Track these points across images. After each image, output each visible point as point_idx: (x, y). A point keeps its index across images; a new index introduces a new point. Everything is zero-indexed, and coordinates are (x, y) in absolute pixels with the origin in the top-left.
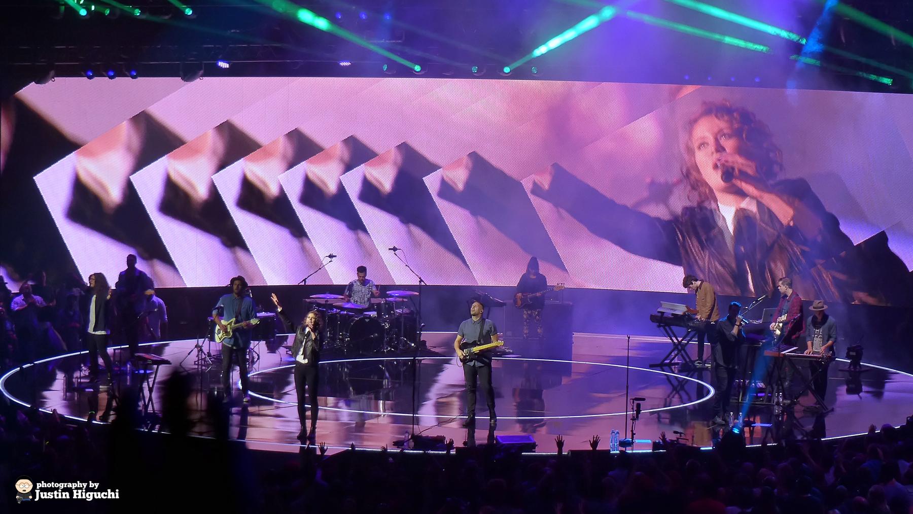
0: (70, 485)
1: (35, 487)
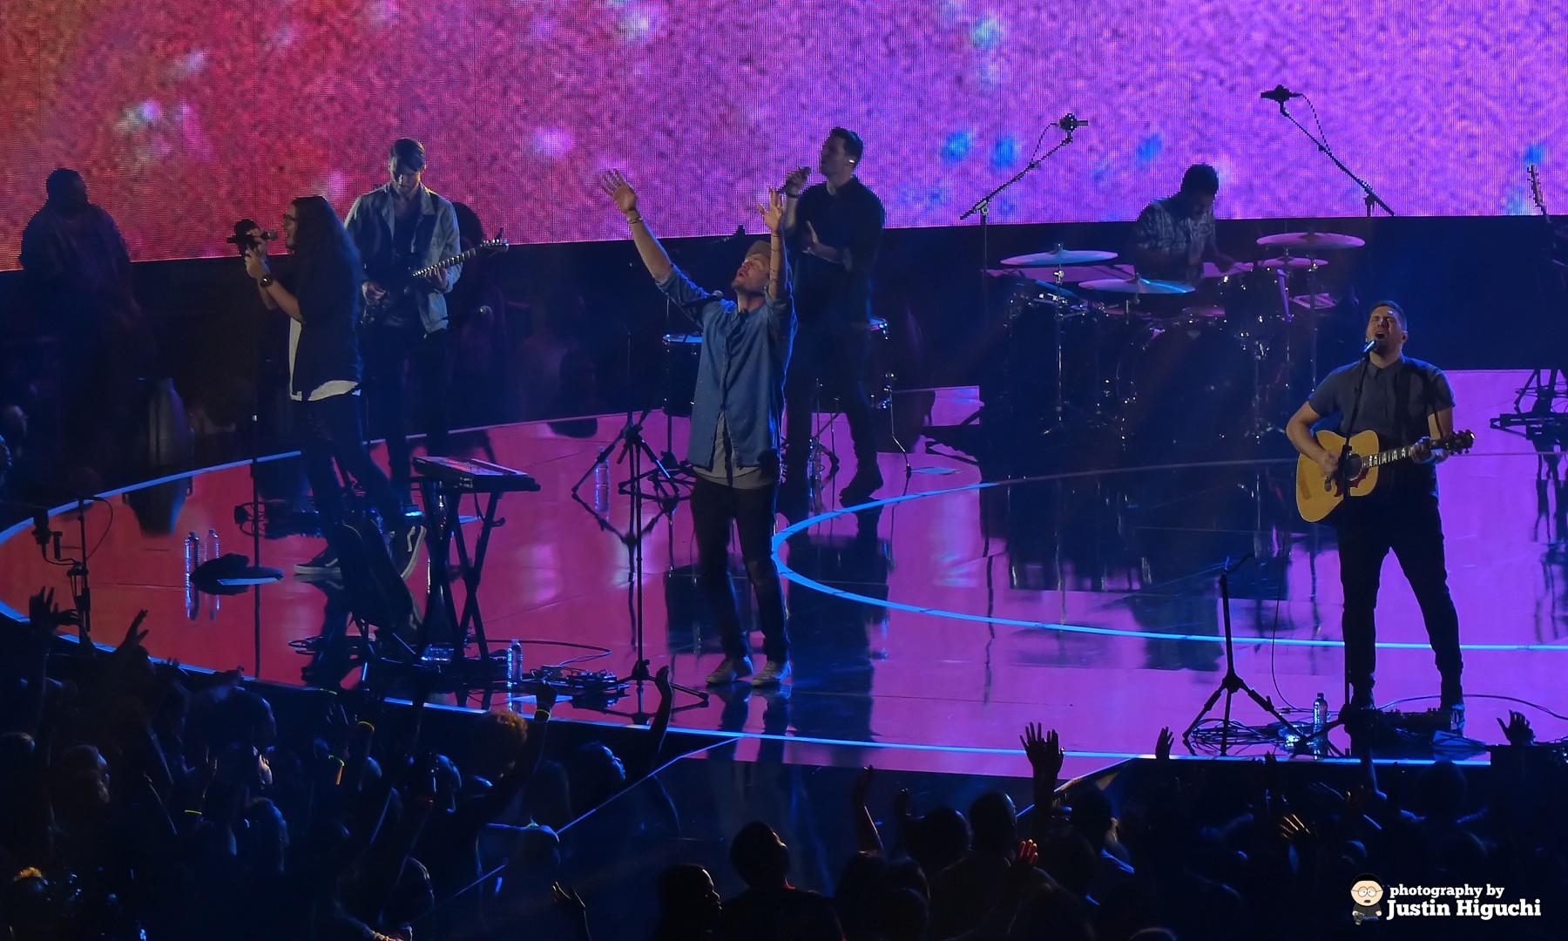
0: (1451, 891)
1: (1386, 895)
